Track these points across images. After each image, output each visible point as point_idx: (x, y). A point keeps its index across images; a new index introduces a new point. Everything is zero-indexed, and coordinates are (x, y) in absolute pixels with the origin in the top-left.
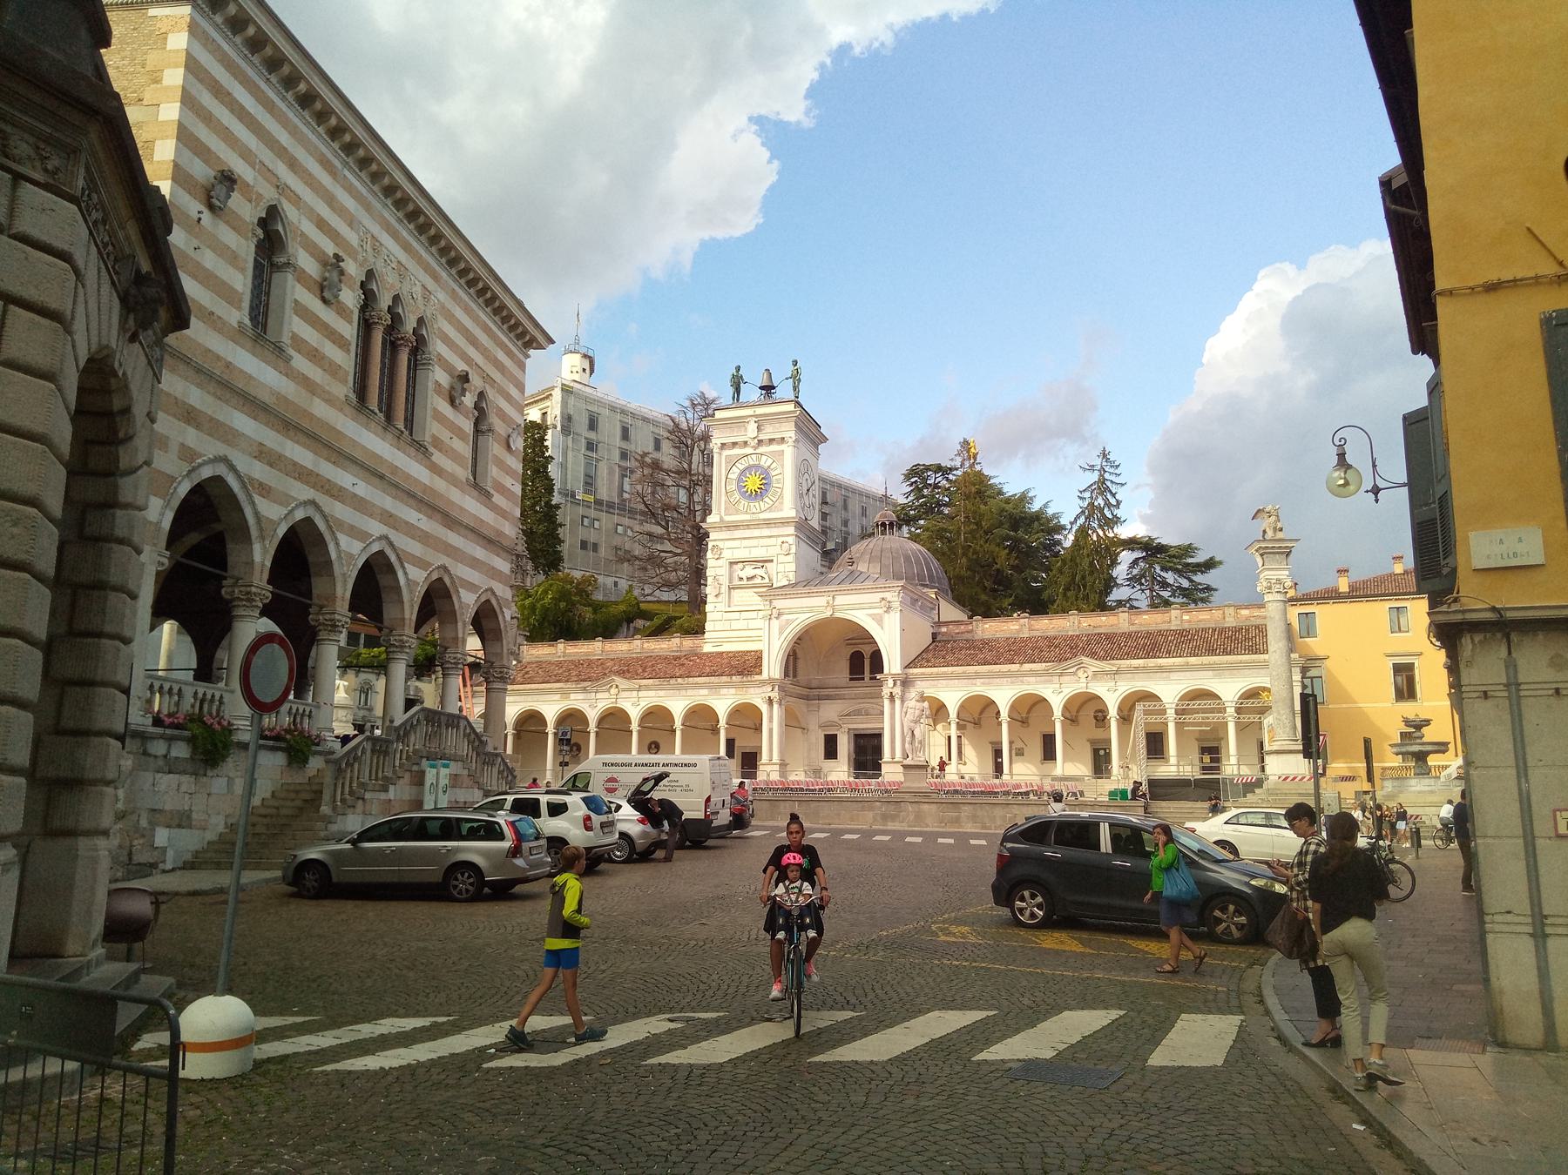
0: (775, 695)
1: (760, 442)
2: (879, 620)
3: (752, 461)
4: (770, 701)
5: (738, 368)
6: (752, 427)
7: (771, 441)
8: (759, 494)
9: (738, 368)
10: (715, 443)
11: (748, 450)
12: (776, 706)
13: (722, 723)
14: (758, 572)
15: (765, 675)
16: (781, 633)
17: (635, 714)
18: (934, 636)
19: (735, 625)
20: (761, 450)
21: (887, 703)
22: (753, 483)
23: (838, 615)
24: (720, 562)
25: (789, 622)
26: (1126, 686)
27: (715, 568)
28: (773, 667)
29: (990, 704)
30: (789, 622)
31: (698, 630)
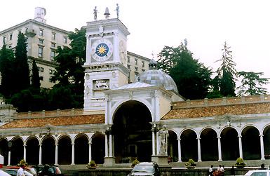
2: (150, 101)
6: (101, 29)
10: (87, 34)
11: (100, 38)
14: (105, 84)
15: (106, 123)
16: (112, 106)
17: (57, 139)
18: (172, 107)
21: (153, 133)
22: (102, 50)
26: (244, 125)
27: (88, 83)
28: (109, 121)
29: (212, 133)
30: (115, 102)
31: (80, 105)
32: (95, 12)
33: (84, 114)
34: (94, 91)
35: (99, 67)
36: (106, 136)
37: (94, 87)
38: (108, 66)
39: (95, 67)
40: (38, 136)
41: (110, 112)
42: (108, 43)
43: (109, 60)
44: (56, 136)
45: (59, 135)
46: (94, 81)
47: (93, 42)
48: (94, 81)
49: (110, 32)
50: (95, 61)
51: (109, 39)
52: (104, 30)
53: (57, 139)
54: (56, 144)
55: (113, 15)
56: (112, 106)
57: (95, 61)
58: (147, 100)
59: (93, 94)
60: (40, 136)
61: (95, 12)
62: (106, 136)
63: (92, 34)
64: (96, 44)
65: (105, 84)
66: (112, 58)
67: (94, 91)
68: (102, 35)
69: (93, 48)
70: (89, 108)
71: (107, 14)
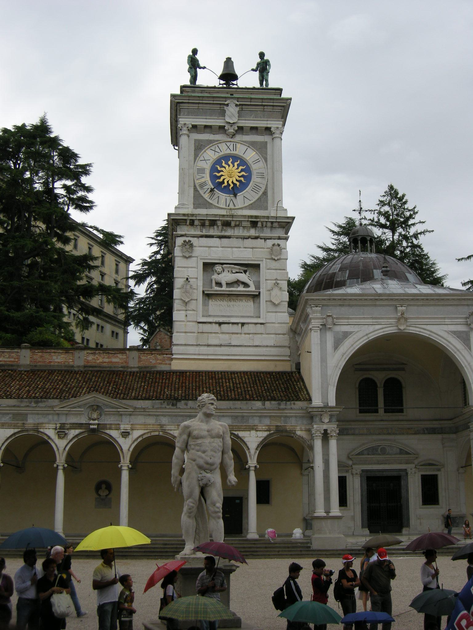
0: (332, 428)
1: (241, 129)
3: (224, 150)
4: (326, 436)
5: (195, 52)
7: (254, 129)
8: (234, 191)
9: (195, 52)
12: (333, 443)
13: (252, 462)
14: (243, 277)
17: (126, 446)
19: (213, 340)
20: (238, 138)
22: (231, 174)
23: (413, 330)
24: (192, 262)
25: (346, 335)
30: (346, 335)
32: (194, 64)
33: (176, 366)
34: (207, 296)
35: (227, 224)
36: (318, 444)
37: (208, 282)
38: (254, 224)
39: (213, 223)
40: (50, 433)
41: (329, 372)
42: (250, 155)
43: (251, 207)
44: (125, 434)
45: (136, 434)
46: (208, 266)
47: (199, 147)
48: (208, 266)
49: (262, 124)
50: (209, 205)
51: (253, 145)
52: (240, 115)
53: (126, 446)
54: (125, 463)
55: (248, 79)
56: (336, 346)
57: (209, 205)
58: (454, 333)
59: (205, 304)
60: (61, 432)
61: (194, 64)
62: (318, 444)
63: (201, 121)
64: (210, 155)
65: (243, 277)
66: (262, 201)
67: (207, 296)
68: (231, 130)
69: (201, 164)
70: (191, 350)
71: (229, 76)
